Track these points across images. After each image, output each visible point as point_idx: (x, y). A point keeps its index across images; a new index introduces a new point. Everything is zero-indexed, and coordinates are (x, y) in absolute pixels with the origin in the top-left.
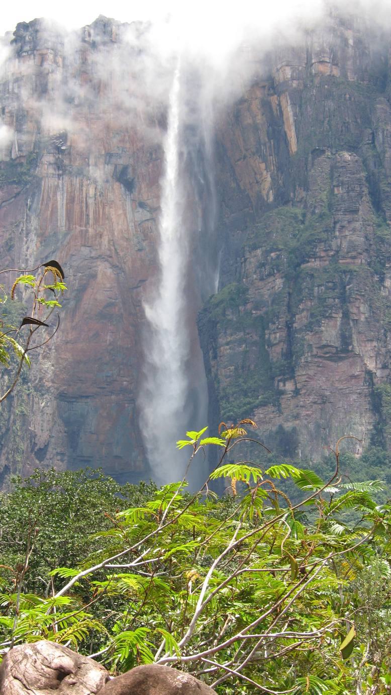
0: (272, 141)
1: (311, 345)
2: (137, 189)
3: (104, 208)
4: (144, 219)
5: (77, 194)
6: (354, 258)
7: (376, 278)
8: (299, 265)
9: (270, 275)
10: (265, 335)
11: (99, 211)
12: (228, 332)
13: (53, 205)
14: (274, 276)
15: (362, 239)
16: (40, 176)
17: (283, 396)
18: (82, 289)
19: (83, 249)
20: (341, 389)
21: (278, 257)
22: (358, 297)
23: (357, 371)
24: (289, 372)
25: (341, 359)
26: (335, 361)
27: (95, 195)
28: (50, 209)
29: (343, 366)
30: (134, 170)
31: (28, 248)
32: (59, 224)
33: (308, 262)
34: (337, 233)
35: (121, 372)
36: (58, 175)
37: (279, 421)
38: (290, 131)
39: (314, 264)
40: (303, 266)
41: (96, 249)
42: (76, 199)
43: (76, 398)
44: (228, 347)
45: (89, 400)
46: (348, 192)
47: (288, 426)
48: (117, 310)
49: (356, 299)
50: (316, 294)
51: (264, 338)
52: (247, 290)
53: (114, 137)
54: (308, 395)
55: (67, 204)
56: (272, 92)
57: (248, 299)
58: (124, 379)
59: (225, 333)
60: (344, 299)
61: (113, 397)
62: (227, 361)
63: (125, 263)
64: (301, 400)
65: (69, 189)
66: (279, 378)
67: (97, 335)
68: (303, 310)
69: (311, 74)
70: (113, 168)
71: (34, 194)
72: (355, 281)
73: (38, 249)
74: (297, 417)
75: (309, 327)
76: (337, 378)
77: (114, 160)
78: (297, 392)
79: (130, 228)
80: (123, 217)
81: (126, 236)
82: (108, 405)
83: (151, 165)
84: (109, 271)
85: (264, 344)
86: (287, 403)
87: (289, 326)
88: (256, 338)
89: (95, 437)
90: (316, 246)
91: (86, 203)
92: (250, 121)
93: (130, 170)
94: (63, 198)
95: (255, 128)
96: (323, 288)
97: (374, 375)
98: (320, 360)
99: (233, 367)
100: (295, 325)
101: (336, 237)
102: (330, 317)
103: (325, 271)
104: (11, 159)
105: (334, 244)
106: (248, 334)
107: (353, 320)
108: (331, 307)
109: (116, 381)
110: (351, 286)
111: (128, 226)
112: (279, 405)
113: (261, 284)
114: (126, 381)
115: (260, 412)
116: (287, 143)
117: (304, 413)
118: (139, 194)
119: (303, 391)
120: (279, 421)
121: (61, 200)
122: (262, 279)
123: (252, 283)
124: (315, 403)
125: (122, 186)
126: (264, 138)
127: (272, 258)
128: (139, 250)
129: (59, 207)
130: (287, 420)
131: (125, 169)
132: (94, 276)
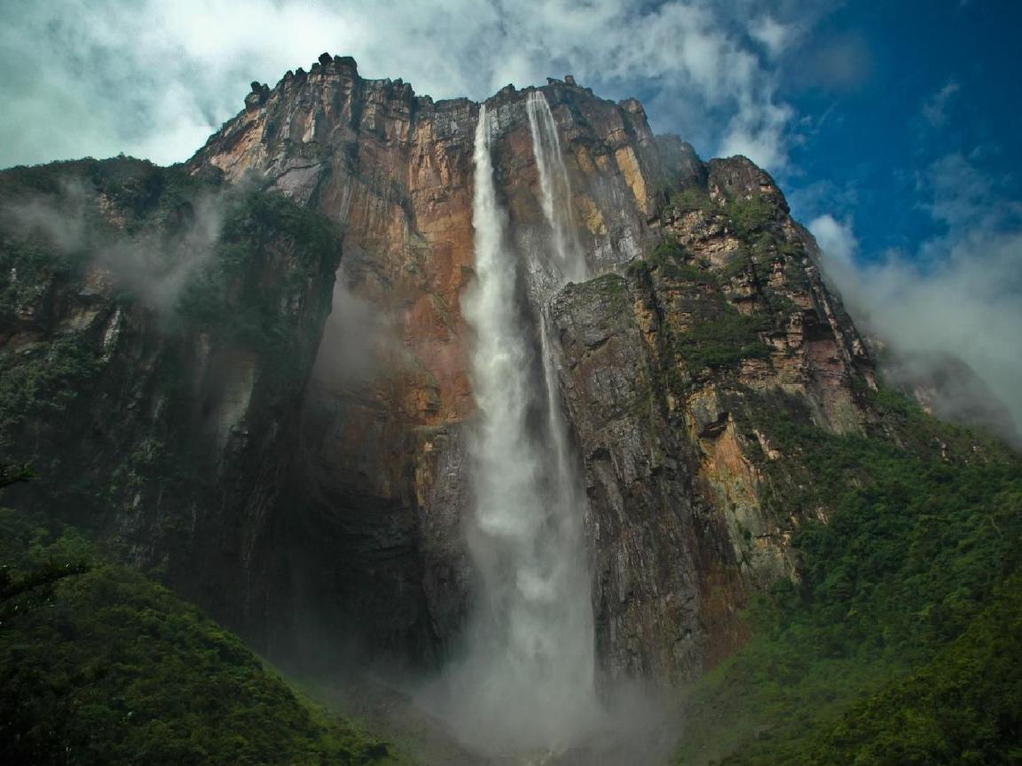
44: (678, 292)
47: (790, 389)
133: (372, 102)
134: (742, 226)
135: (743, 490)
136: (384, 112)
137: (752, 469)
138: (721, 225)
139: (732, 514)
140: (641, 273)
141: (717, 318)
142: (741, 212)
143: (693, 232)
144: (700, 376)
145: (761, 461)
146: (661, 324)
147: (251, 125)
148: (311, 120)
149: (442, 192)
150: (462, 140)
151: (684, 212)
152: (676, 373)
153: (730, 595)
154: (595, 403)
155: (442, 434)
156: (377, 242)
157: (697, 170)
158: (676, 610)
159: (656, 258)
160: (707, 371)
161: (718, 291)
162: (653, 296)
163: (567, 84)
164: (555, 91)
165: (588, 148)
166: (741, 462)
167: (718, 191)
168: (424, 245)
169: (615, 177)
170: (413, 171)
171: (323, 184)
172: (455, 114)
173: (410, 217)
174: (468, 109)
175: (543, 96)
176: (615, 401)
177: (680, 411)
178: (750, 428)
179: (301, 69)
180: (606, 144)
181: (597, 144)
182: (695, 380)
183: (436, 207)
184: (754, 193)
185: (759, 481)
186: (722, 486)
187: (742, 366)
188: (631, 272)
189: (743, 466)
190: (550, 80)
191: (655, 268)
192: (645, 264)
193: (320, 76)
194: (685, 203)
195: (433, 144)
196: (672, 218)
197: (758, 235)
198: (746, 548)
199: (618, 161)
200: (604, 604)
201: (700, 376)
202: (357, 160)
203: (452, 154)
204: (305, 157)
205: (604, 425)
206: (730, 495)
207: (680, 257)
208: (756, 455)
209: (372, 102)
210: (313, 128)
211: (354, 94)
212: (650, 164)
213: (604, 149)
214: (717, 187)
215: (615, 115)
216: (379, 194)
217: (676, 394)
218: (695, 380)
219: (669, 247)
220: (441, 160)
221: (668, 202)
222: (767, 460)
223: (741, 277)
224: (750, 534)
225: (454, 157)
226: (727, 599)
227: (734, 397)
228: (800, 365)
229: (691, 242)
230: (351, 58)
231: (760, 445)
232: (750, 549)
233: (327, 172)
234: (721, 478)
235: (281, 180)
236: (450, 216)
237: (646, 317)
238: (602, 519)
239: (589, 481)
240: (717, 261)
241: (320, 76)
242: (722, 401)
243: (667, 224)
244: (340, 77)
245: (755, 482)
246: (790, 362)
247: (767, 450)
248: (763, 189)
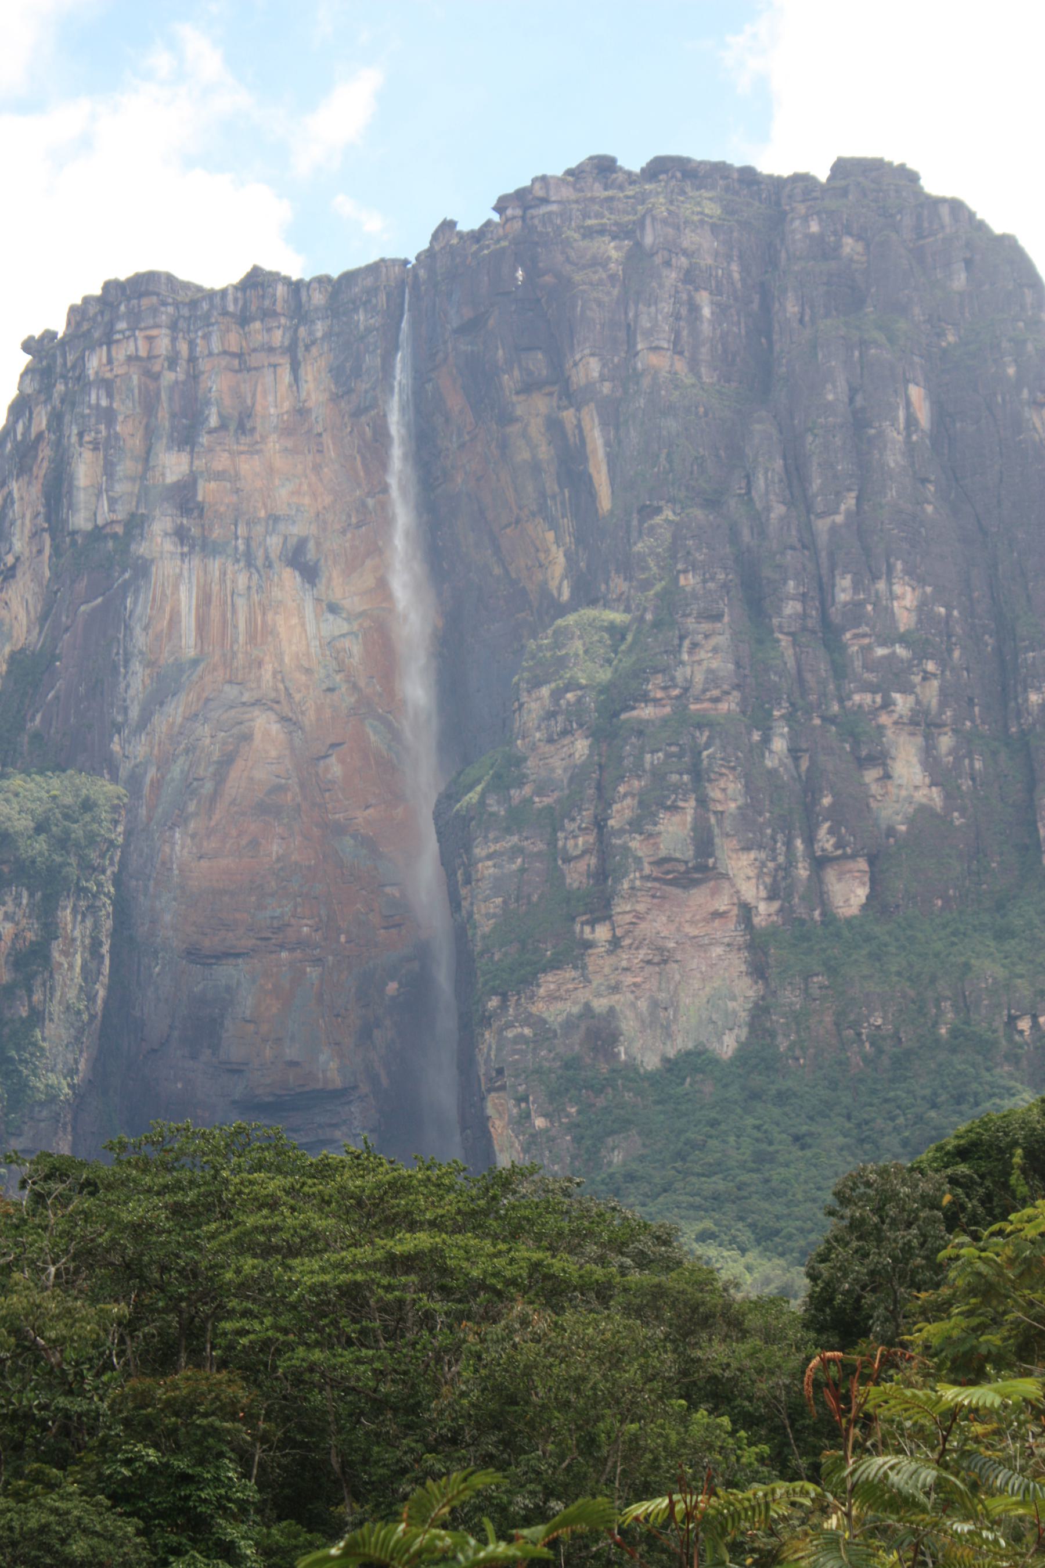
0: (566, 491)
1: (640, 858)
2: (324, 580)
3: (264, 614)
4: (337, 633)
5: (215, 588)
6: (716, 700)
7: (756, 736)
8: (616, 714)
9: (565, 733)
10: (557, 840)
12: (491, 836)
15: (731, 666)
16: (149, 557)
17: (590, 951)
18: (228, 760)
19: (227, 688)
20: (695, 937)
21: (579, 700)
22: (724, 770)
23: (722, 903)
24: (600, 909)
25: (695, 883)
26: (685, 887)
27: (249, 588)
28: (167, 616)
29: (700, 899)
30: (318, 544)
31: (128, 686)
33: (634, 708)
34: (685, 657)
35: (299, 910)
36: (182, 554)
37: (583, 995)
38: (599, 472)
39: (646, 712)
40: (624, 716)
41: (252, 689)
42: (214, 598)
43: (217, 957)
44: (490, 863)
45: (240, 961)
46: (704, 581)
47: (600, 1005)
48: (289, 798)
49: (722, 775)
50: (647, 766)
51: (555, 846)
52: (525, 759)
53: (283, 486)
54: (637, 948)
56: (565, 402)
57: (525, 776)
58: (305, 921)
59: (486, 837)
60: (699, 776)
61: (284, 955)
63: (303, 713)
64: (624, 958)
65: (202, 581)
66: (584, 918)
67: (254, 844)
68: (625, 796)
69: (635, 369)
70: (281, 540)
71: (137, 591)
72: (717, 742)
73: (144, 687)
74: (615, 989)
75: (636, 826)
76: (688, 916)
77: (281, 527)
78: (615, 943)
79: (313, 650)
81: (305, 664)
82: (275, 970)
83: (349, 535)
84: (275, 728)
85: (556, 856)
86: (599, 962)
87: (600, 824)
88: (541, 846)
89: (251, 1027)
90: (647, 681)
91: (233, 605)
92: (526, 455)
93: (311, 545)
94: (190, 597)
95: (536, 468)
96: (661, 754)
97: (754, 912)
98: (657, 885)
99: (500, 899)
100: (611, 822)
101: (682, 663)
102: (674, 808)
103: (665, 721)
104: (96, 526)
105: (679, 674)
106: (527, 839)
107: (715, 813)
108: (675, 788)
109: (289, 925)
110: (711, 750)
111: (308, 645)
112: (584, 967)
113: (548, 748)
116: (592, 495)
117: (629, 979)
118: (328, 588)
119: (627, 942)
120: (583, 995)
121: (187, 600)
122: (550, 741)
123: (534, 748)
124: (649, 962)
125: (297, 574)
126: (551, 486)
127: (568, 703)
128: (330, 690)
130: (599, 995)
131: (302, 543)
132: (247, 737)
141: (535, 898)
160: (494, 1003)
171: (139, 609)
187: (539, 986)
202: (196, 514)
216: (249, 564)
227: (520, 1038)
228: (624, 964)
246: (611, 960)
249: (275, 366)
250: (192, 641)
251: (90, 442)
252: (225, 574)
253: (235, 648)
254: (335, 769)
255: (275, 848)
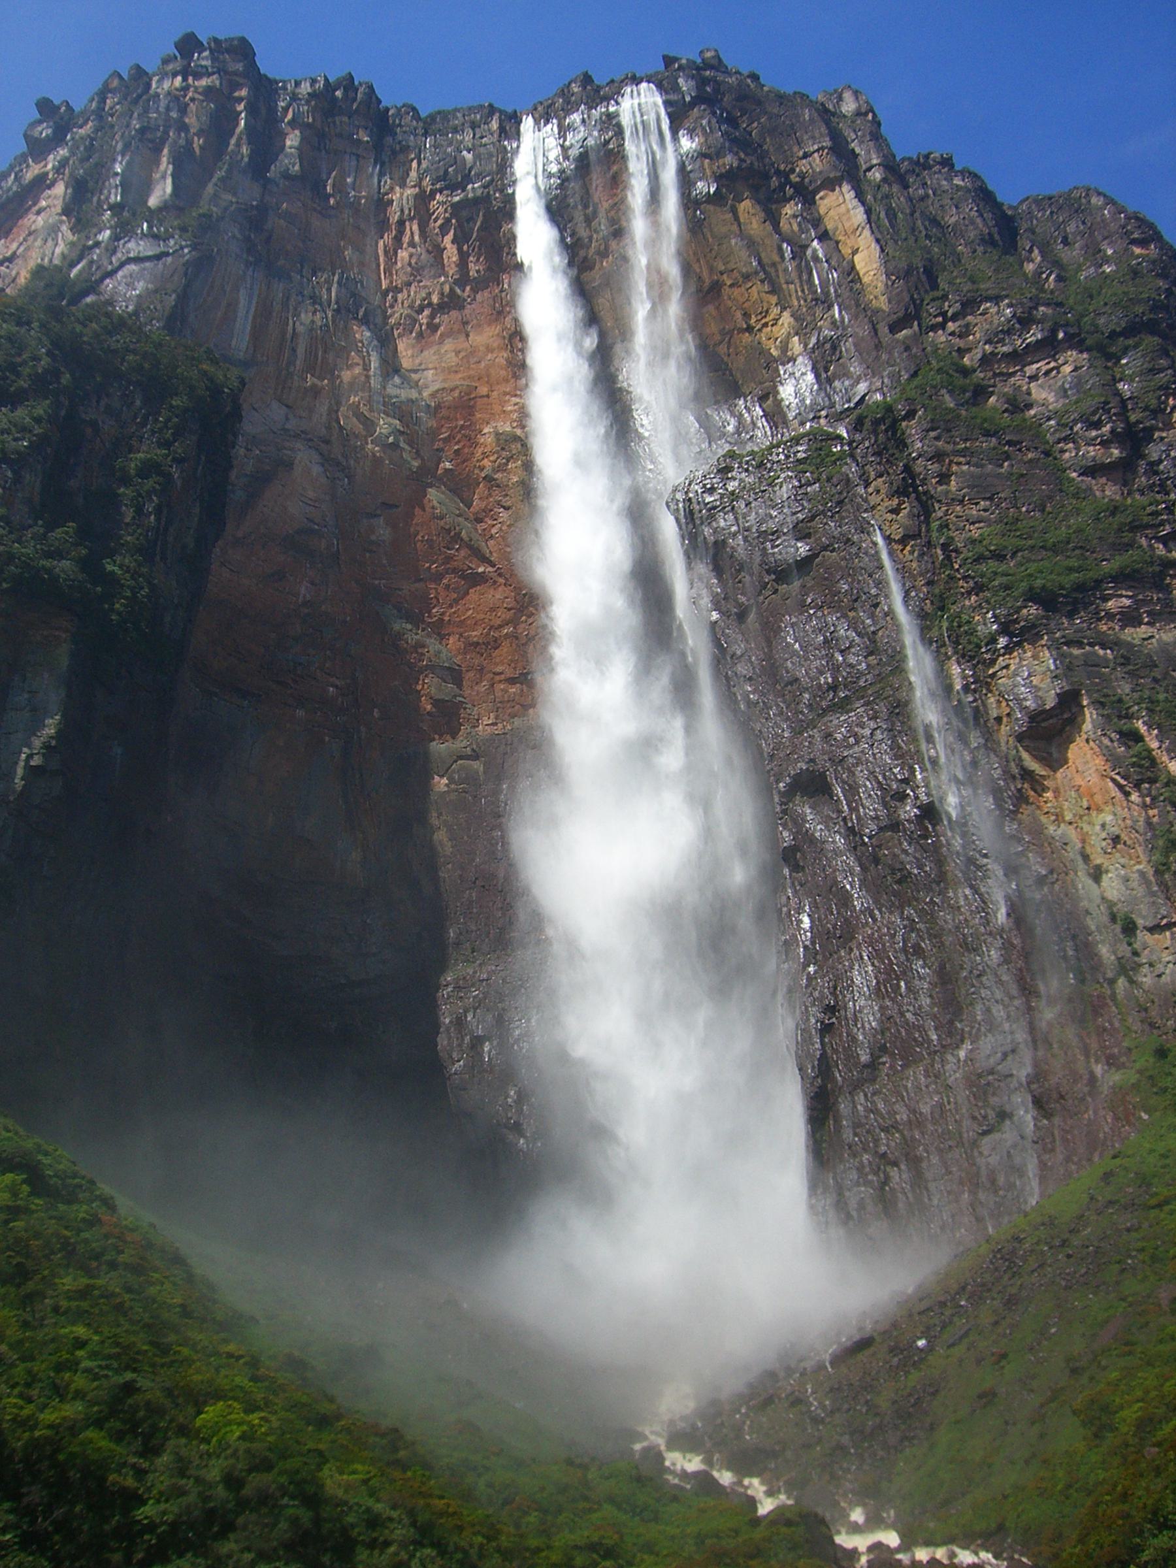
3: (325, 352)
11: (316, 356)
13: (229, 305)
14: (1054, 348)
27: (313, 322)
32: (234, 343)
44: (962, 459)
55: (254, 318)
61: (300, 713)
62: (968, 487)
80: (363, 378)
84: (316, 470)
114: (337, 687)
115: (1124, 593)
129: (240, 314)
133: (293, 123)
134: (1096, 326)
135: (1116, 840)
136: (317, 140)
137: (1134, 797)
138: (1048, 325)
139: (1095, 886)
140: (882, 428)
142: (1091, 297)
143: (988, 342)
144: (1016, 621)
145: (1152, 781)
146: (928, 524)
147: (41, 183)
148: (165, 164)
149: (447, 288)
150: (484, 187)
151: (969, 305)
152: (965, 617)
153: (1094, 1046)
154: (791, 683)
155: (468, 757)
156: (316, 392)
157: (991, 223)
158: (980, 1076)
159: (912, 394)
160: (1032, 611)
161: (1047, 454)
162: (907, 469)
163: (707, 65)
164: (681, 81)
165: (755, 189)
166: (1111, 784)
167: (1039, 258)
168: (414, 394)
169: (815, 243)
170: (386, 252)
172: (468, 136)
173: (386, 341)
174: (494, 125)
175: (657, 93)
176: (835, 678)
177: (975, 691)
178: (1129, 717)
179: (138, 67)
180: (794, 178)
181: (775, 182)
182: (1005, 630)
183: (437, 320)
184: (1117, 259)
185: (1148, 818)
186: (1072, 834)
187: (1105, 599)
188: (858, 426)
189: (1115, 792)
190: (669, 61)
191: (910, 415)
192: (889, 409)
193: (179, 78)
194: (969, 286)
195: (423, 199)
196: (944, 314)
197: (1131, 342)
198: (1124, 950)
199: (822, 211)
200: (824, 1067)
201: (1016, 621)
203: (464, 213)
204: (156, 237)
205: (812, 724)
206: (1088, 850)
207: (964, 390)
208: (1140, 773)
209: (293, 123)
210: (169, 181)
211: (252, 110)
212: (891, 214)
213: (789, 191)
214: (1036, 251)
215: (811, 120)
217: (965, 657)
218: (1005, 630)
219: (939, 371)
220: (441, 227)
221: (934, 286)
222: (1163, 778)
223: (1097, 425)
224: (1134, 923)
225: (472, 219)
226: (1086, 1052)
229: (986, 360)
230: (243, 41)
231: (1150, 751)
232: (1136, 953)
233: (202, 264)
234: (1067, 818)
235: (109, 284)
236: (467, 336)
237: (896, 511)
238: (815, 906)
239: (785, 834)
240: (1043, 395)
241: (179, 78)
242: (1067, 668)
243: (934, 328)
244: (221, 78)
245: (1141, 824)
247: (1165, 758)
248: (1138, 251)
249: (358, 156)
250: (244, 346)
251: (152, 141)
252: (288, 299)
253: (292, 369)
254: (383, 532)
255: (303, 590)
